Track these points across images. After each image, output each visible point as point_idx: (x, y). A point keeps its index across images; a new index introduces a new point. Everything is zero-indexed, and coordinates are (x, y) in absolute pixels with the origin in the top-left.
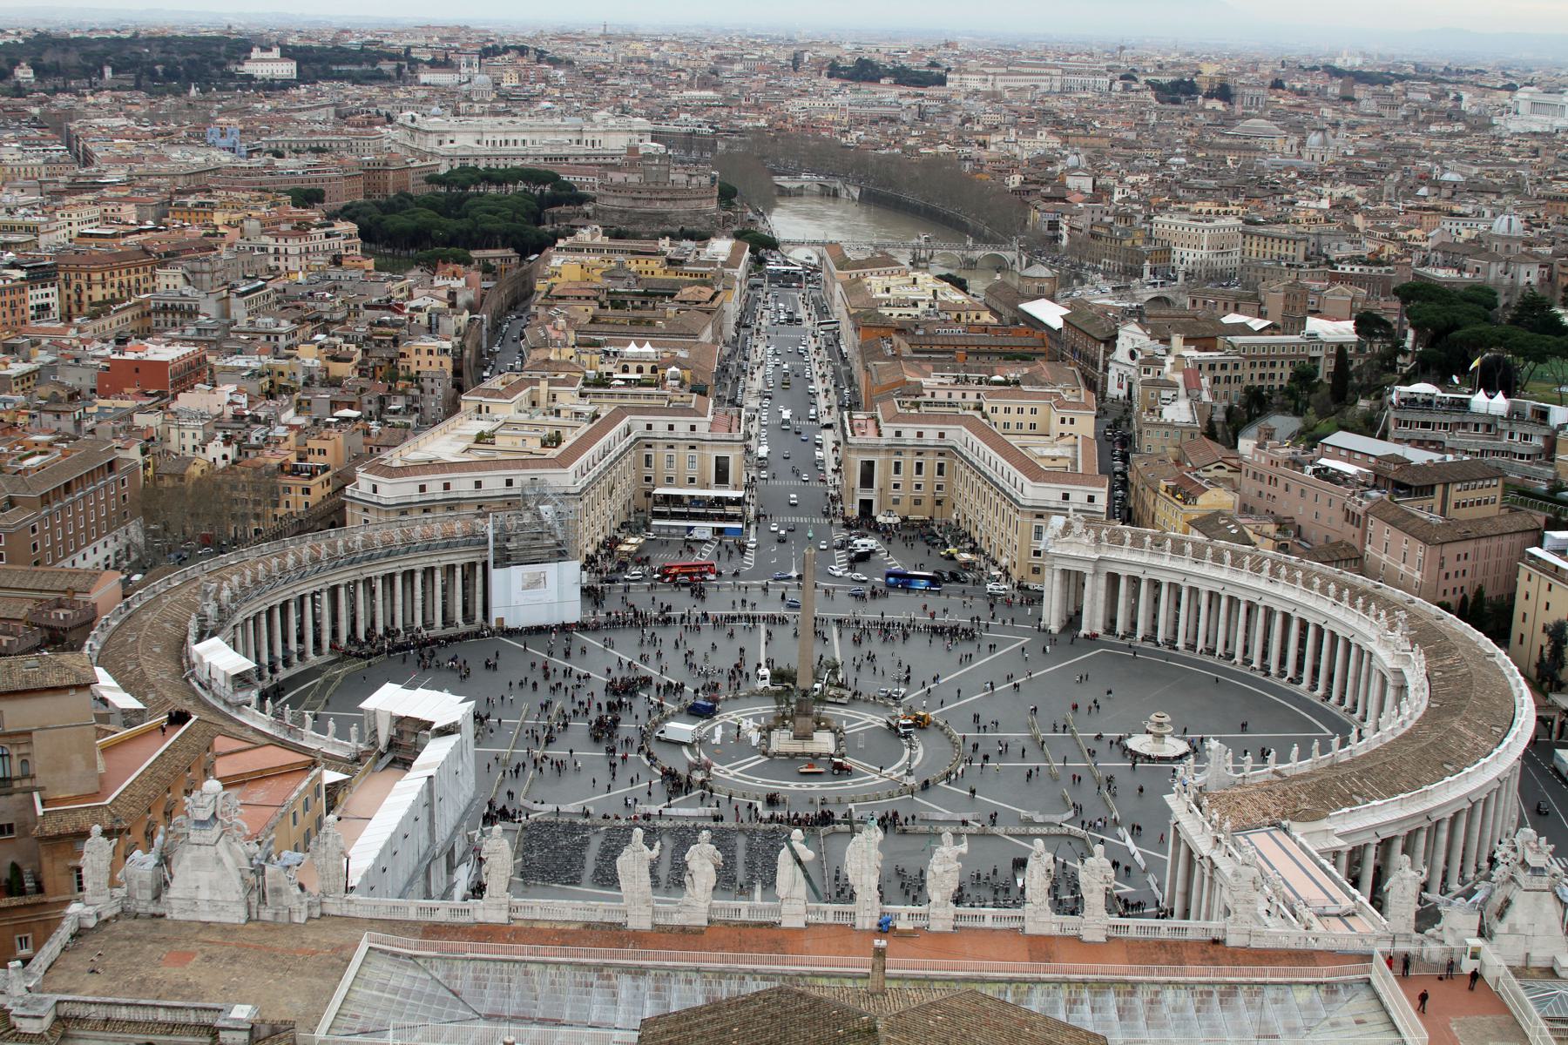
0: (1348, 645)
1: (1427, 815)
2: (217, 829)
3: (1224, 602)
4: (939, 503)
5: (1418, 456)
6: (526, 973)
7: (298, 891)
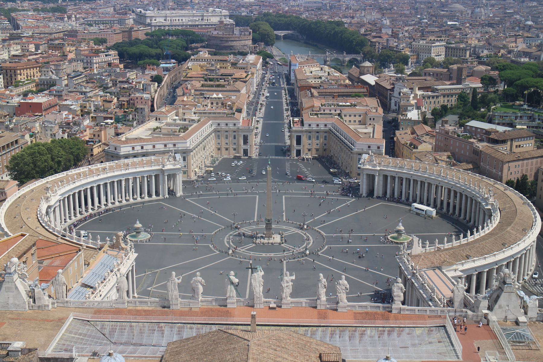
0: (472, 200)
1: (496, 263)
2: (16, 276)
3: (426, 185)
4: (325, 150)
5: (501, 129)
6: (131, 326)
7: (48, 298)
